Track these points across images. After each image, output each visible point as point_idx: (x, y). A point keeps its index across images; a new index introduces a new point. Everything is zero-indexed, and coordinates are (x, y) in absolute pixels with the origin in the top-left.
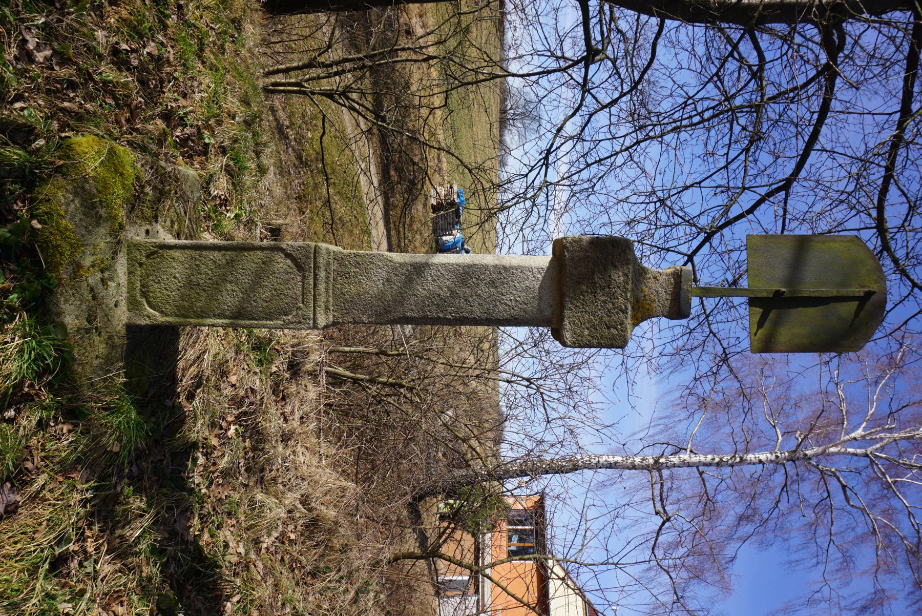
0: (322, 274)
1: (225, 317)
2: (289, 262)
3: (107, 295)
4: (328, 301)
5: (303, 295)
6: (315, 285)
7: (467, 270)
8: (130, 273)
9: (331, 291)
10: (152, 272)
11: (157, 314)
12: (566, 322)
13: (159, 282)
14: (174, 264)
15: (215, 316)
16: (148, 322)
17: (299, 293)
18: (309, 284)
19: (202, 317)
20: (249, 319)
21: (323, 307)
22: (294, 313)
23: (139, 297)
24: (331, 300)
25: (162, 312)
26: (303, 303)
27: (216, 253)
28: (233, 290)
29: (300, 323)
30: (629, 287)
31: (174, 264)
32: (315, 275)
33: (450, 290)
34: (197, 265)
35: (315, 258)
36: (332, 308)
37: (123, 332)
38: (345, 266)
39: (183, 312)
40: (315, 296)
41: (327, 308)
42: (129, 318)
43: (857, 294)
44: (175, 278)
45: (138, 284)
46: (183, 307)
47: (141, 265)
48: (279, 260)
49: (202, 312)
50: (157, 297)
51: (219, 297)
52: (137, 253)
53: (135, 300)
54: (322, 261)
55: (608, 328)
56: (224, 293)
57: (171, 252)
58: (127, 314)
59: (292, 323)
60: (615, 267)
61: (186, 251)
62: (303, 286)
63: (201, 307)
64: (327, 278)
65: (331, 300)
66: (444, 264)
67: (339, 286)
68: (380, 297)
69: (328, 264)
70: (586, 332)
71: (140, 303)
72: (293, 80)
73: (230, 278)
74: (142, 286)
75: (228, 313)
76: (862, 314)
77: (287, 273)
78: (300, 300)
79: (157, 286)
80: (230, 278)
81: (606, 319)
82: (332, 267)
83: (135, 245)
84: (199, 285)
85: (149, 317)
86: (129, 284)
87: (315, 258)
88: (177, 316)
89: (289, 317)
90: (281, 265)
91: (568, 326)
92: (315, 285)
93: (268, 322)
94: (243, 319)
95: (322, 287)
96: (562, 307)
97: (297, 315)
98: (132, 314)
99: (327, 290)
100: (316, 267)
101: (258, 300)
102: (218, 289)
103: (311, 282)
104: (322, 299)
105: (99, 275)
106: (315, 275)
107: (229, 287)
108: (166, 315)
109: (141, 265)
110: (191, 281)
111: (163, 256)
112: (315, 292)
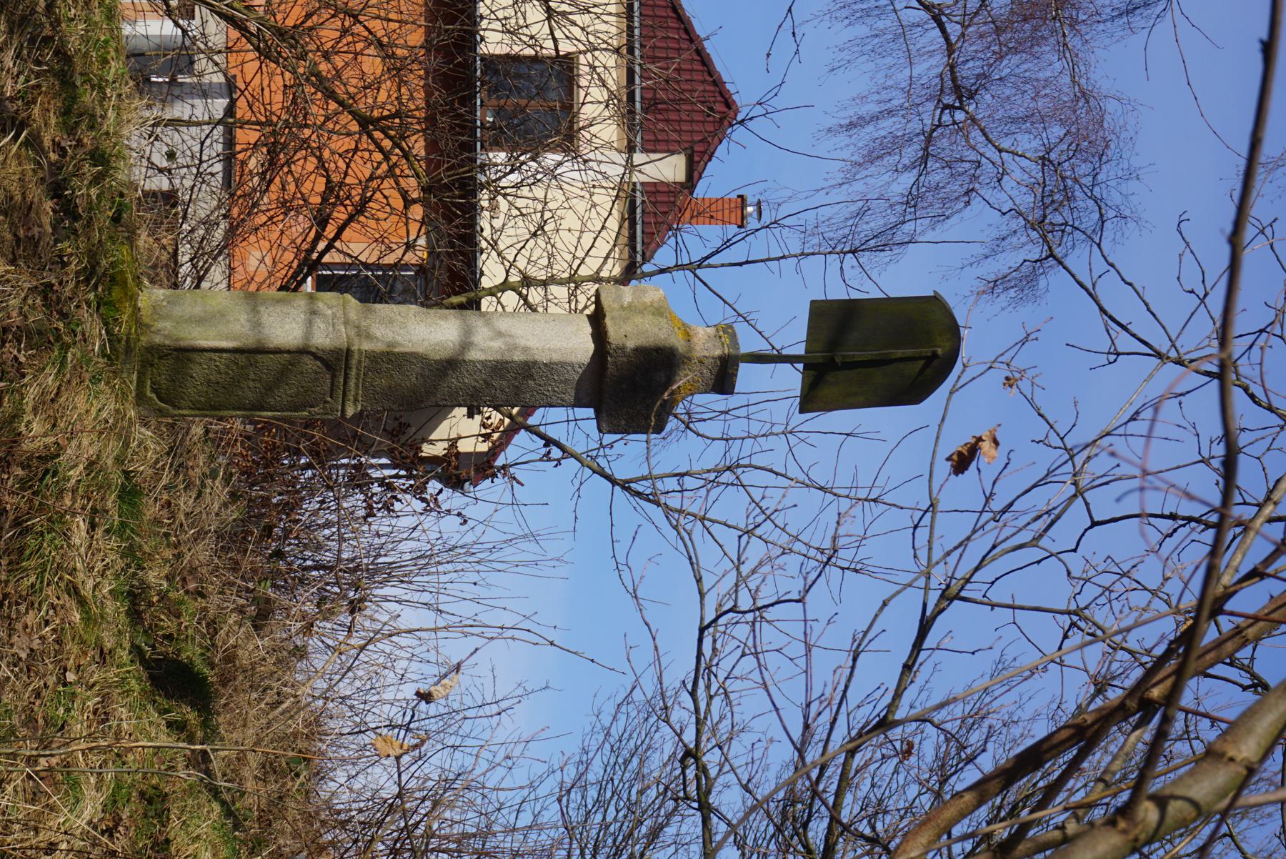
0: (353, 373)
1: (245, 409)
2: (319, 363)
4: (357, 394)
6: (345, 382)
7: (505, 365)
11: (170, 408)
15: (234, 409)
19: (220, 410)
21: (352, 398)
23: (149, 394)
24: (360, 392)
26: (331, 397)
33: (485, 381)
35: (347, 360)
38: (377, 363)
41: (356, 400)
43: (924, 354)
48: (308, 362)
51: (240, 393)
54: (354, 362)
62: (332, 384)
64: (358, 374)
65: (360, 392)
66: (482, 362)
69: (360, 362)
75: (248, 406)
76: (928, 371)
77: (316, 373)
80: (252, 376)
84: (218, 383)
87: (347, 360)
89: (316, 409)
92: (345, 382)
95: (352, 384)
97: (324, 408)
99: (357, 385)
100: (348, 367)
103: (342, 380)
107: (251, 384)
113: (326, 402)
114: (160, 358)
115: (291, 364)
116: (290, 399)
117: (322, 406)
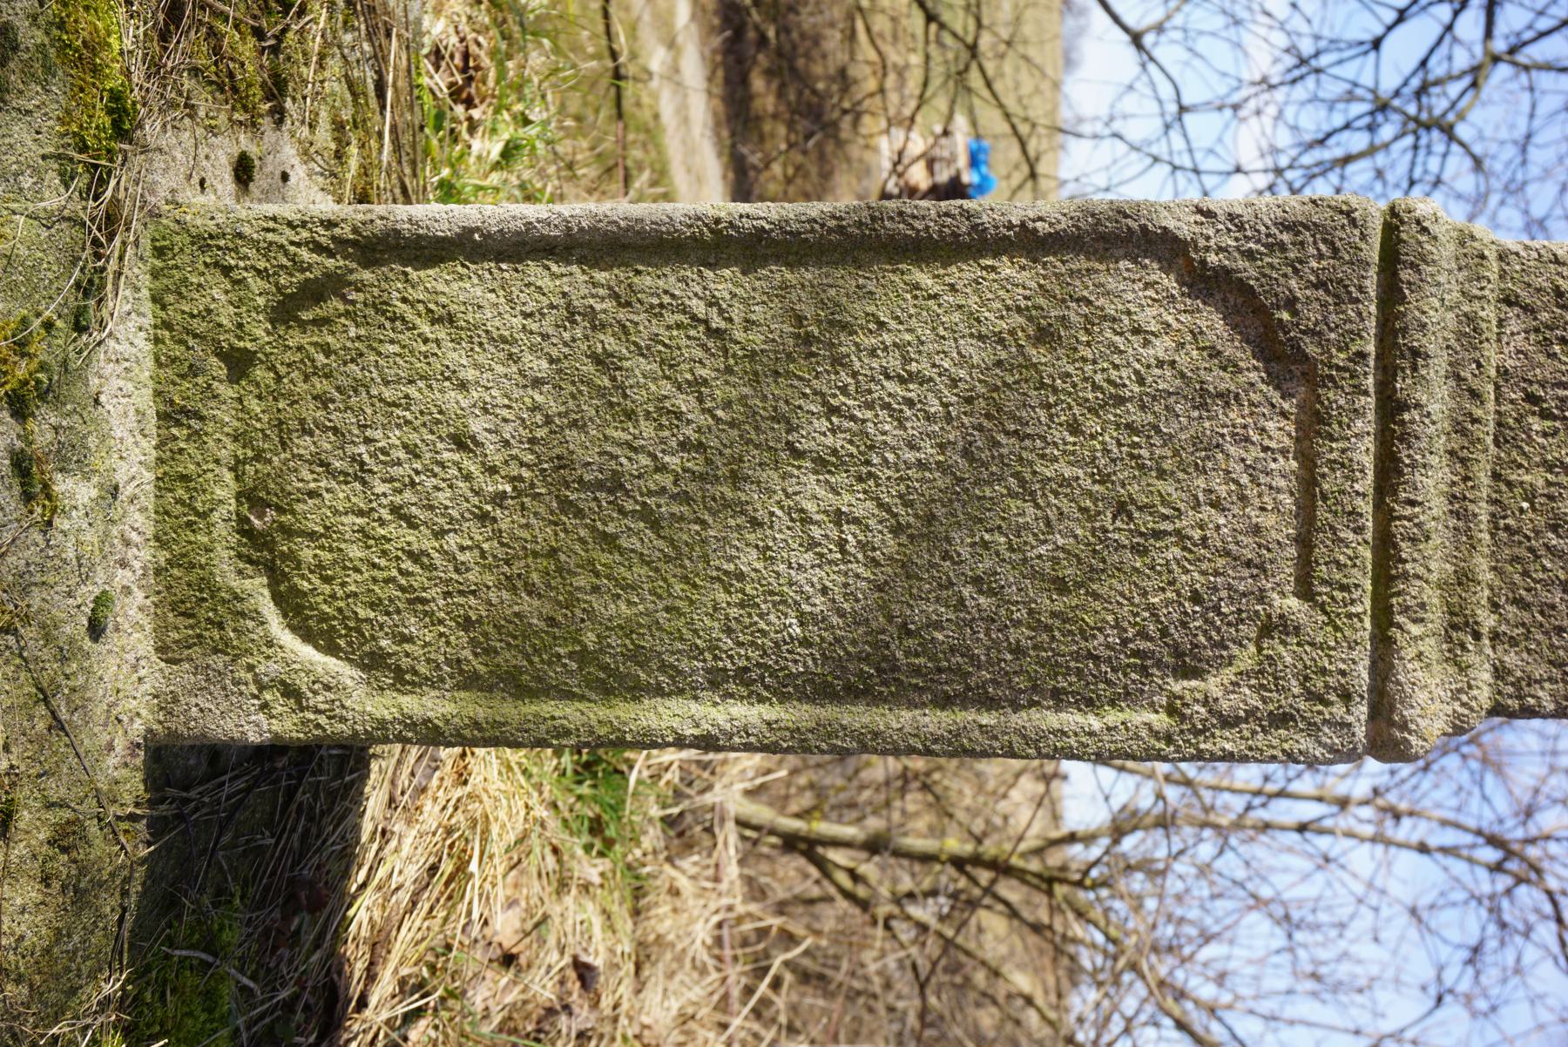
2: (1212, 322)
3: (50, 561)
4: (1464, 578)
5: (1304, 542)
6: (1389, 471)
8: (171, 415)
9: (1483, 511)
10: (311, 412)
13: (361, 473)
14: (455, 356)
16: (285, 724)
17: (1280, 528)
18: (1349, 469)
19: (637, 692)
20: (945, 702)
22: (1246, 658)
23: (226, 570)
25: (373, 662)
26: (1305, 591)
27: (725, 282)
28: (839, 517)
29: (1282, 719)
31: (455, 356)
32: (1391, 408)
34: (602, 361)
35: (1391, 294)
36: (1488, 621)
37: (133, 786)
39: (508, 658)
40: (1385, 546)
41: (1459, 624)
42: (166, 703)
44: (461, 442)
45: (224, 489)
46: (516, 630)
47: (239, 364)
48: (1148, 317)
49: (638, 656)
50: (344, 563)
51: (749, 560)
52: (218, 292)
53: (207, 586)
56: (783, 533)
57: (438, 282)
58: (154, 675)
59: (1228, 722)
61: (533, 270)
62: (1308, 484)
63: (628, 630)
64: (1462, 426)
65: (1482, 566)
67: (1537, 479)
71: (240, 611)
74: (251, 497)
75: (802, 662)
77: (1203, 399)
78: (1286, 571)
79: (342, 494)
80: (817, 434)
82: (1492, 356)
83: (203, 242)
84: (615, 484)
85: (290, 692)
86: (164, 484)
87: (1391, 294)
88: (470, 682)
89: (1213, 685)
90: (1161, 347)
92: (1389, 471)
93: (1071, 719)
94: (903, 696)
98: (184, 675)
101: (1007, 575)
102: (739, 508)
103: (1365, 454)
106: (1391, 408)
107: (812, 492)
108: (403, 679)
109: (239, 364)
110: (562, 463)
111: (380, 307)
112: (1385, 515)
113: (1270, 627)
114: (284, 312)
115: (1044, 336)
116: (1047, 603)
117: (1246, 658)
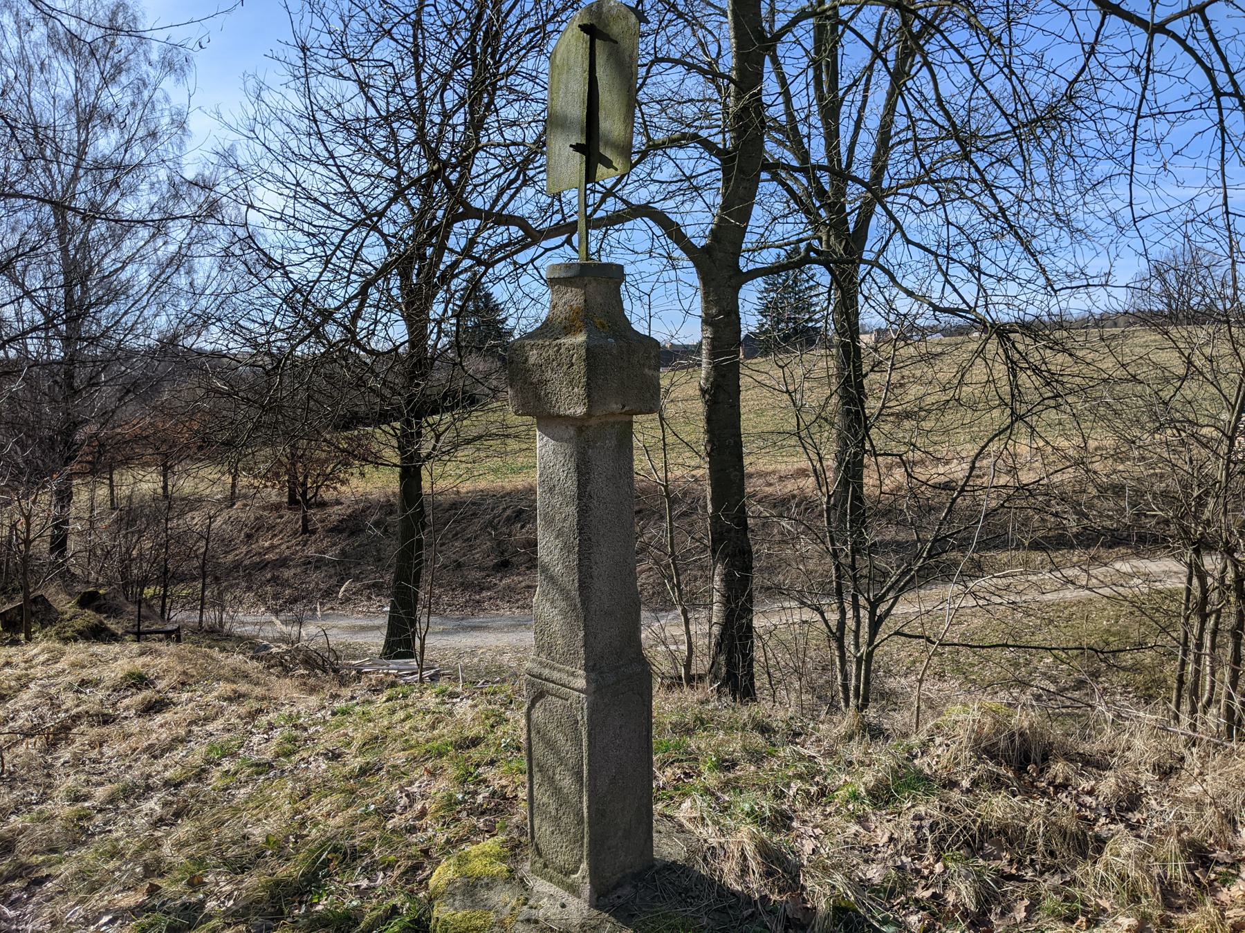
0: (546, 672)
2: (538, 705)
12: (568, 412)
15: (581, 803)
16: (587, 880)
21: (571, 678)
30: (540, 342)
32: (546, 680)
33: (557, 537)
37: (596, 912)
41: (573, 674)
55: (572, 365)
60: (527, 360)
68: (564, 613)
69: (541, 663)
70: (576, 390)
72: (854, 667)
73: (550, 773)
81: (565, 367)
91: (572, 411)
95: (556, 675)
96: (559, 416)
99: (560, 671)
100: (539, 677)
104: (565, 678)
105: (525, 908)
109: (546, 866)
